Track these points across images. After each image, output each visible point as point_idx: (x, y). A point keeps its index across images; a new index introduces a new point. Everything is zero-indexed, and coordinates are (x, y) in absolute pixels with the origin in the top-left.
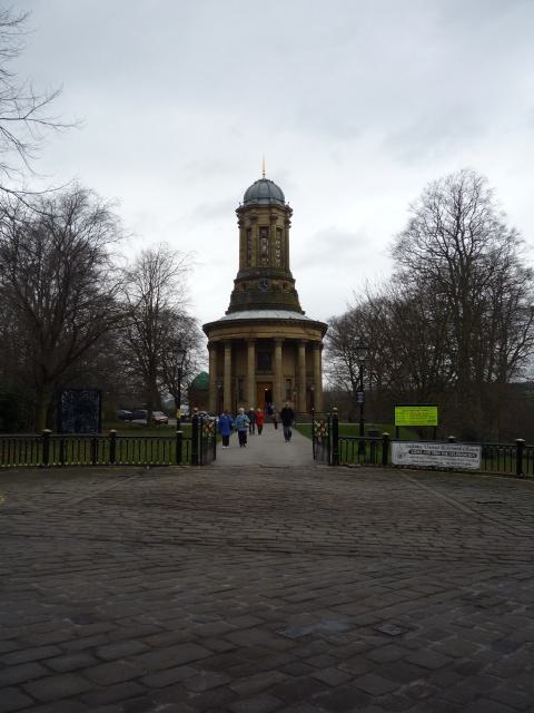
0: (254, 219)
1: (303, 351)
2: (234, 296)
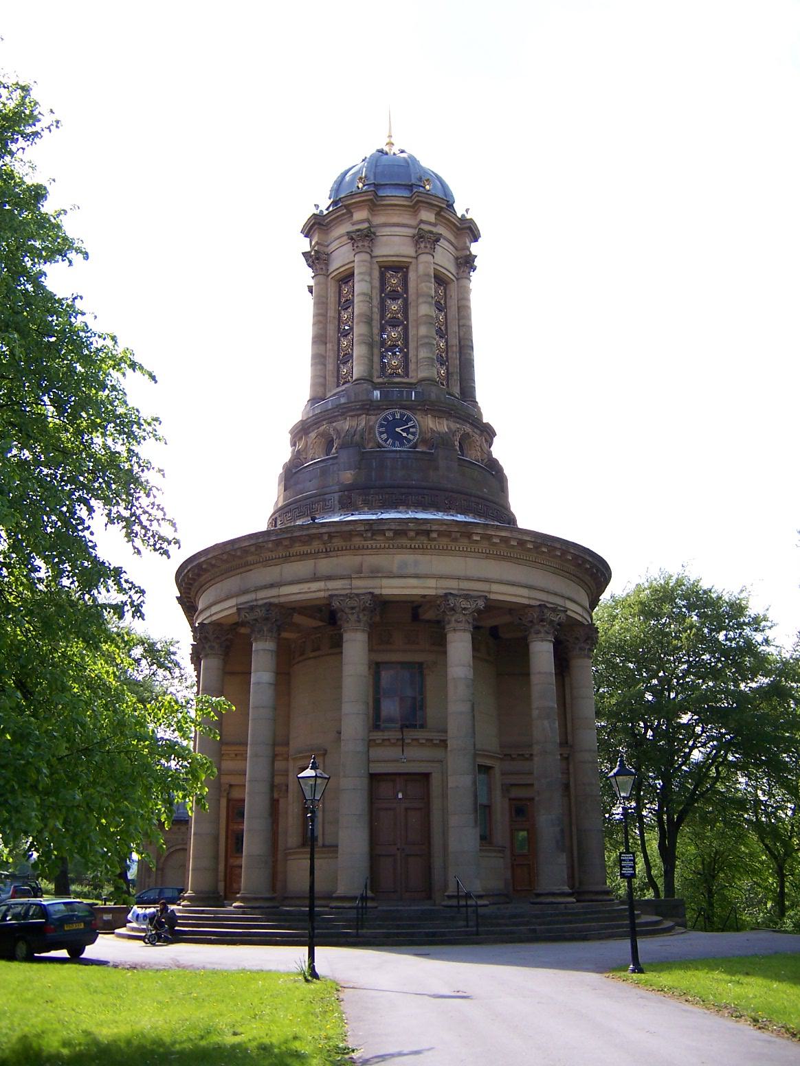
0: (364, 238)
1: (542, 653)
2: (292, 475)
